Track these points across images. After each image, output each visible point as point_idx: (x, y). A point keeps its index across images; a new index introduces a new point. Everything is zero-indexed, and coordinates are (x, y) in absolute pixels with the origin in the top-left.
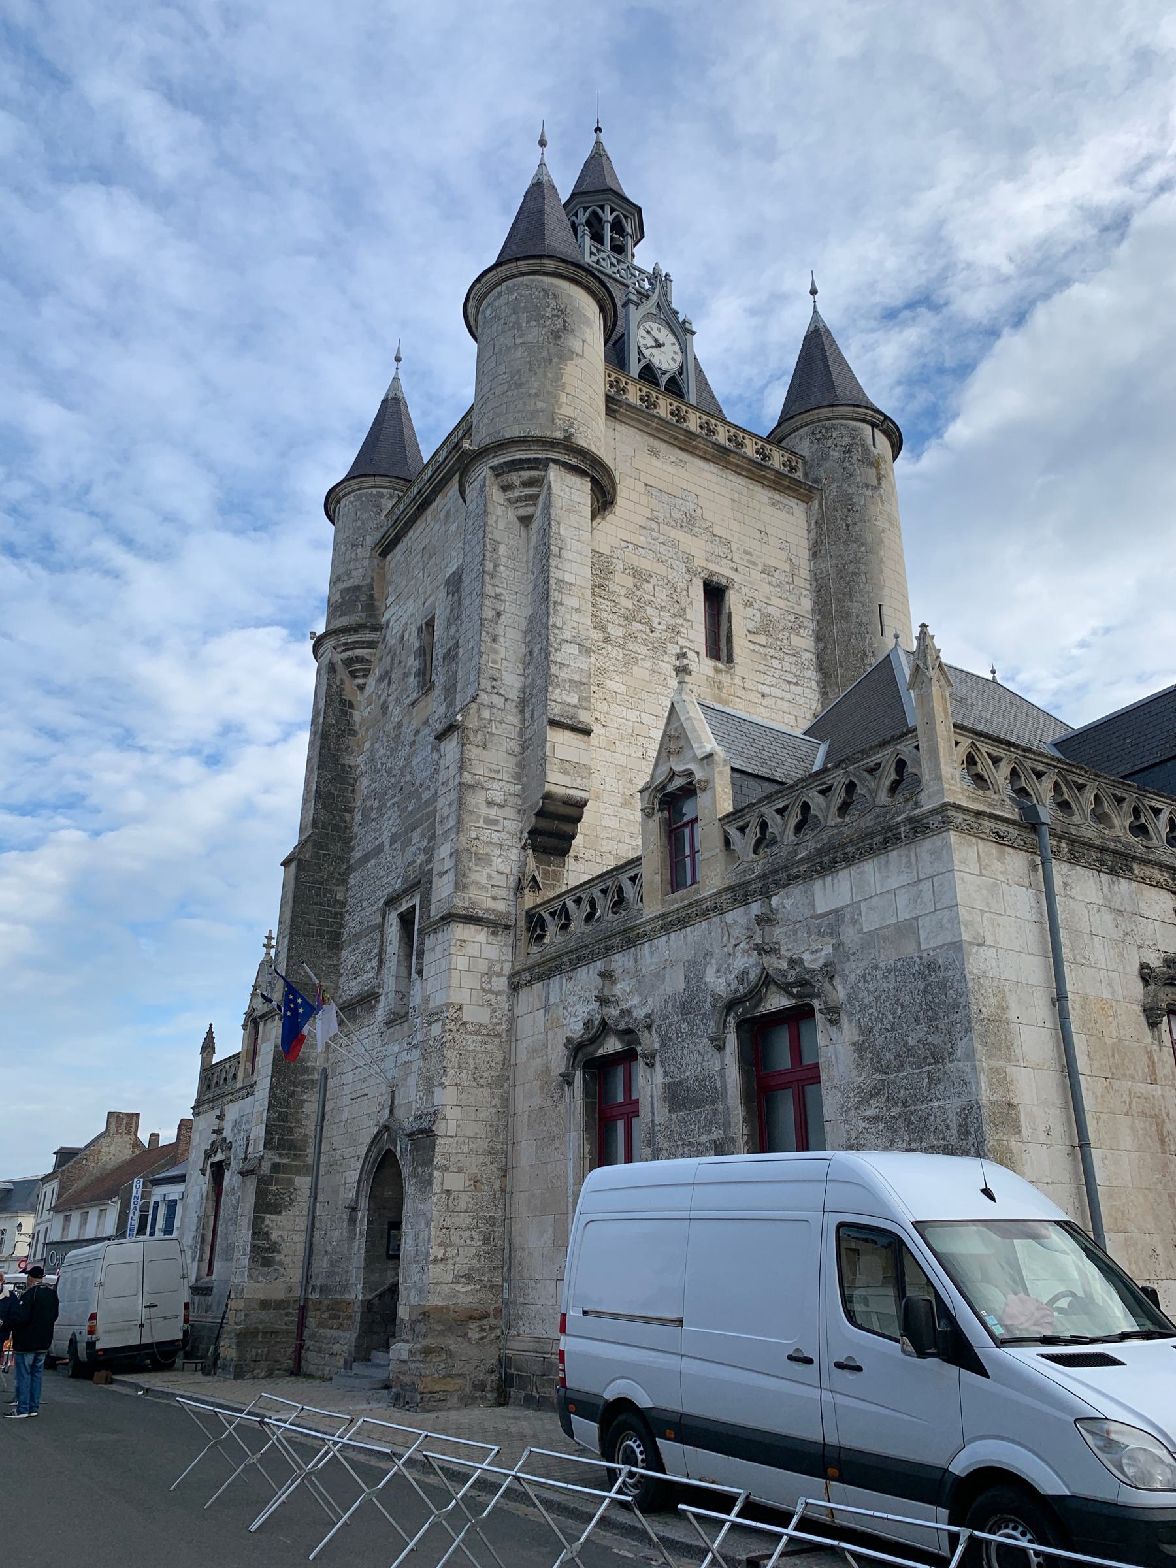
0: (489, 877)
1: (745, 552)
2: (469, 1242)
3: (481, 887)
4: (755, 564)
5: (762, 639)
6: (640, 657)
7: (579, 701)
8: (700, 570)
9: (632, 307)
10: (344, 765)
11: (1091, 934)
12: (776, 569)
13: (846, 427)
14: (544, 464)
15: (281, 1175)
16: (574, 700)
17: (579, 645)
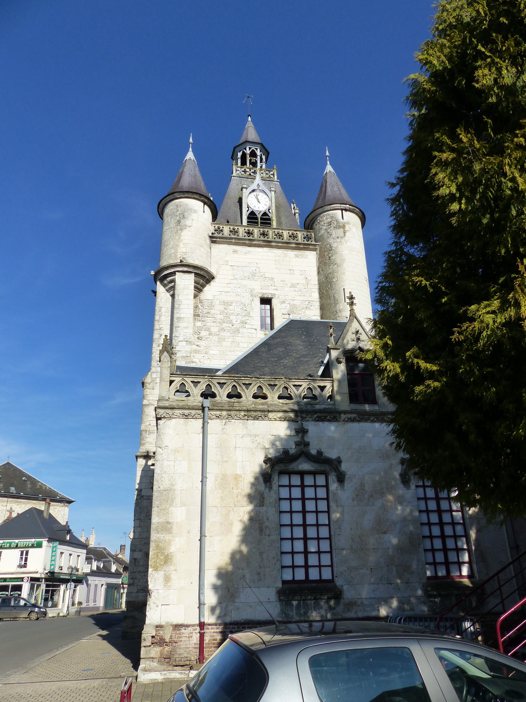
1: (282, 281)
6: (226, 337)
8: (257, 294)
9: (244, 190)
11: (236, 447)
13: (329, 214)
14: (174, 273)
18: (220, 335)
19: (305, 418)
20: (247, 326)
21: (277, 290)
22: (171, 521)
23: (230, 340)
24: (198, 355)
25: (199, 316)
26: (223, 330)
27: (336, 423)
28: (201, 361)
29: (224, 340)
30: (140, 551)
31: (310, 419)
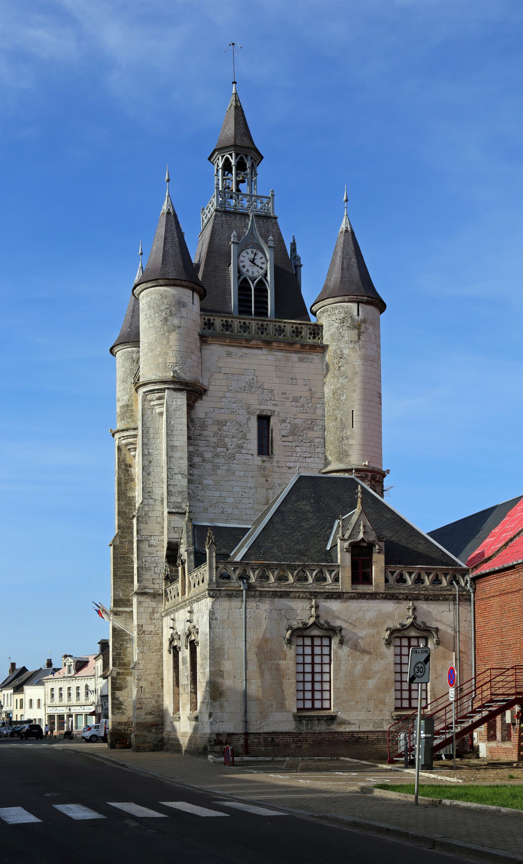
0: (151, 576)
1: (283, 394)
2: (150, 702)
3: (148, 580)
4: (288, 398)
5: (290, 438)
7: (182, 500)
10: (129, 497)
12: (301, 397)
15: (121, 676)
16: (180, 500)
17: (182, 474)
18: (214, 462)
19: (317, 596)
20: (244, 451)
21: (276, 405)
22: (222, 670)
23: (225, 467)
24: (192, 485)
25: (191, 439)
26: (217, 455)
27: (340, 600)
28: (195, 492)
29: (218, 467)
30: (145, 680)
31: (321, 597)
